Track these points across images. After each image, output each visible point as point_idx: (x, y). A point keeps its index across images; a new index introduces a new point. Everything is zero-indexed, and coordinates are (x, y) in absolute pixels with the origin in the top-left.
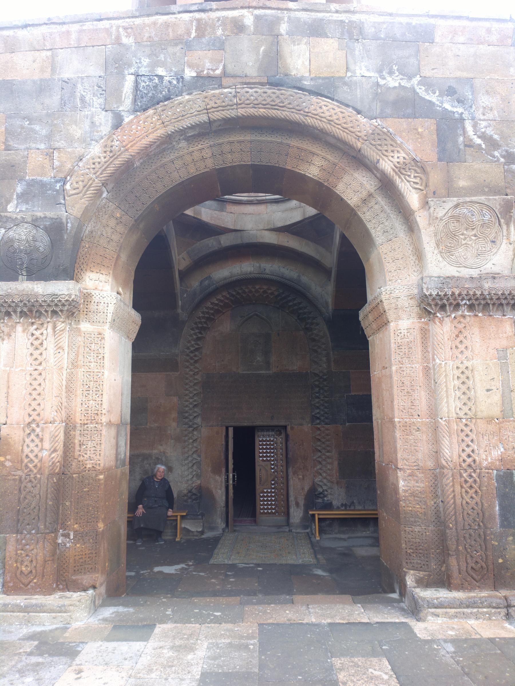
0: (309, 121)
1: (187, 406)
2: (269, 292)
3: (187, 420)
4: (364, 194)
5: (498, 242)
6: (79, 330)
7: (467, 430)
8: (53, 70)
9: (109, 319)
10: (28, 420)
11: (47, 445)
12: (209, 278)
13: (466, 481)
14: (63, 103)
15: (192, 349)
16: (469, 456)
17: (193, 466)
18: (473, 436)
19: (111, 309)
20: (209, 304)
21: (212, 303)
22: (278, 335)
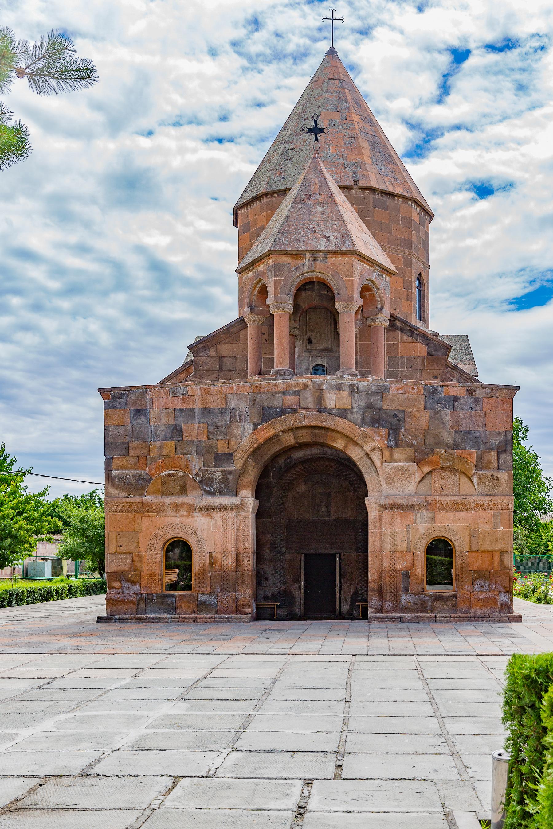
0: (335, 428)
1: (276, 540)
2: (330, 466)
3: (277, 549)
4: (359, 457)
5: (410, 482)
6: (240, 515)
7: (393, 556)
8: (226, 404)
9: (251, 510)
10: (222, 551)
11: (230, 560)
12: (290, 457)
13: (391, 575)
14: (231, 419)
15: (279, 503)
16: (393, 566)
17: (280, 578)
18: (395, 558)
19: (252, 506)
20: (290, 474)
21: (292, 474)
22: (336, 494)
